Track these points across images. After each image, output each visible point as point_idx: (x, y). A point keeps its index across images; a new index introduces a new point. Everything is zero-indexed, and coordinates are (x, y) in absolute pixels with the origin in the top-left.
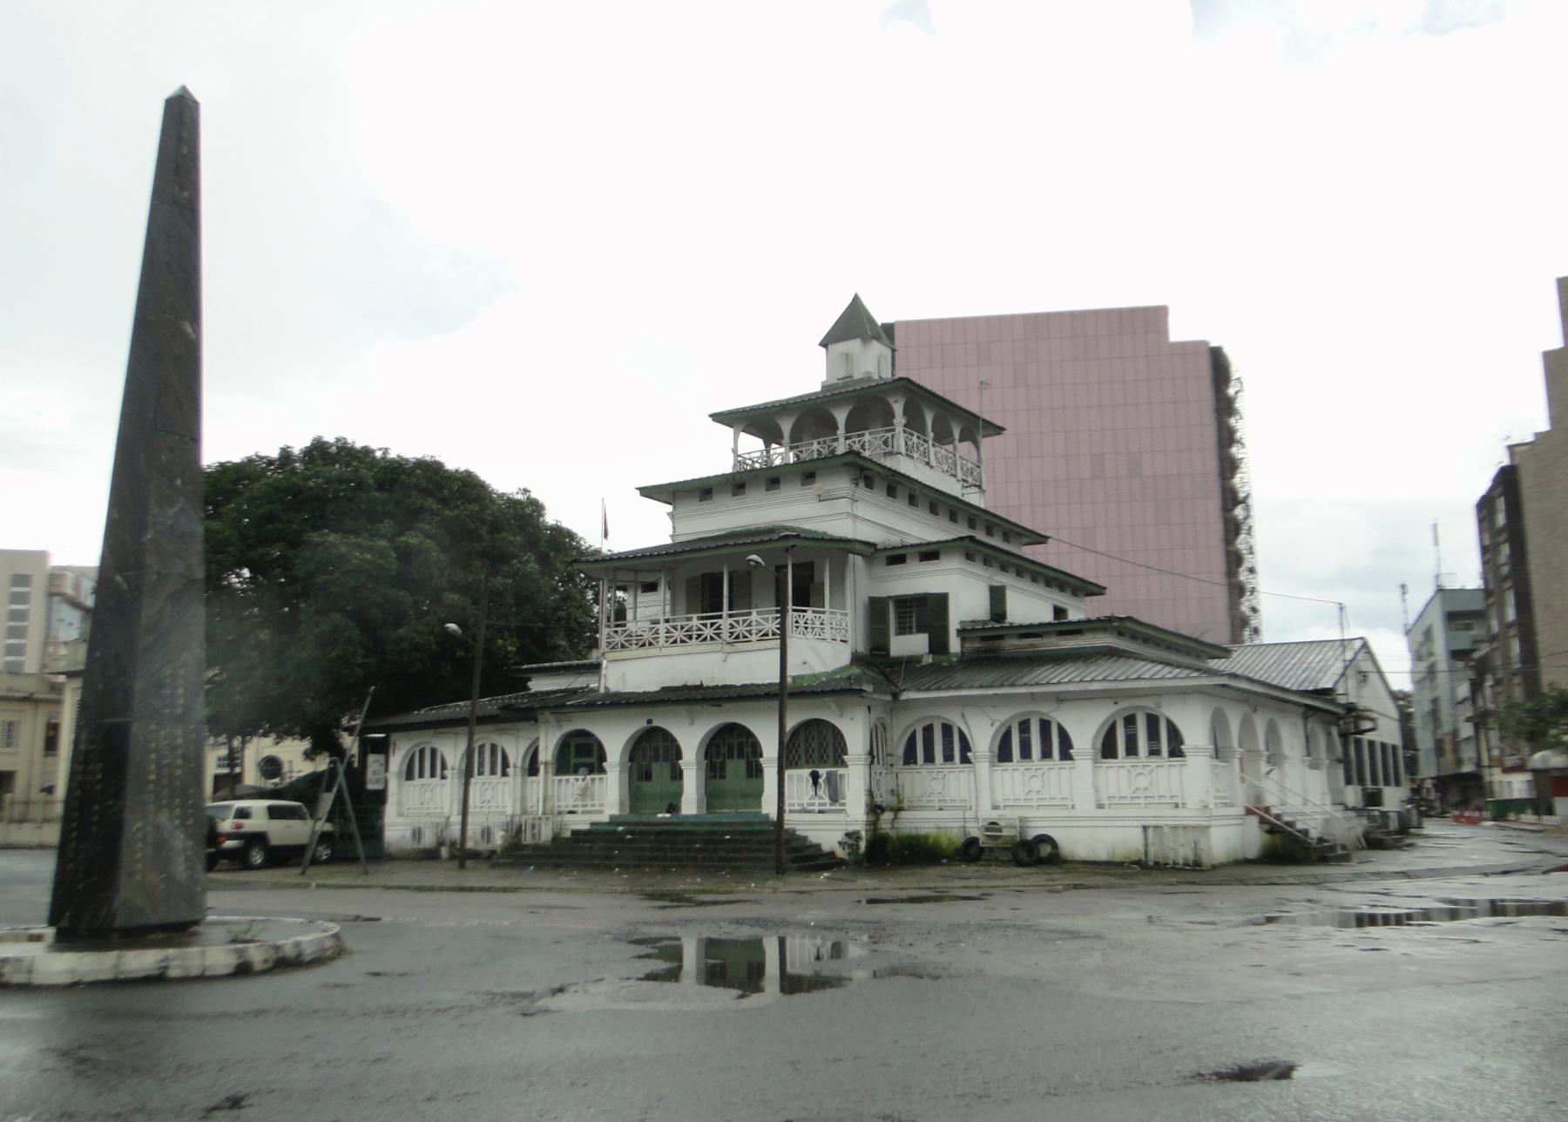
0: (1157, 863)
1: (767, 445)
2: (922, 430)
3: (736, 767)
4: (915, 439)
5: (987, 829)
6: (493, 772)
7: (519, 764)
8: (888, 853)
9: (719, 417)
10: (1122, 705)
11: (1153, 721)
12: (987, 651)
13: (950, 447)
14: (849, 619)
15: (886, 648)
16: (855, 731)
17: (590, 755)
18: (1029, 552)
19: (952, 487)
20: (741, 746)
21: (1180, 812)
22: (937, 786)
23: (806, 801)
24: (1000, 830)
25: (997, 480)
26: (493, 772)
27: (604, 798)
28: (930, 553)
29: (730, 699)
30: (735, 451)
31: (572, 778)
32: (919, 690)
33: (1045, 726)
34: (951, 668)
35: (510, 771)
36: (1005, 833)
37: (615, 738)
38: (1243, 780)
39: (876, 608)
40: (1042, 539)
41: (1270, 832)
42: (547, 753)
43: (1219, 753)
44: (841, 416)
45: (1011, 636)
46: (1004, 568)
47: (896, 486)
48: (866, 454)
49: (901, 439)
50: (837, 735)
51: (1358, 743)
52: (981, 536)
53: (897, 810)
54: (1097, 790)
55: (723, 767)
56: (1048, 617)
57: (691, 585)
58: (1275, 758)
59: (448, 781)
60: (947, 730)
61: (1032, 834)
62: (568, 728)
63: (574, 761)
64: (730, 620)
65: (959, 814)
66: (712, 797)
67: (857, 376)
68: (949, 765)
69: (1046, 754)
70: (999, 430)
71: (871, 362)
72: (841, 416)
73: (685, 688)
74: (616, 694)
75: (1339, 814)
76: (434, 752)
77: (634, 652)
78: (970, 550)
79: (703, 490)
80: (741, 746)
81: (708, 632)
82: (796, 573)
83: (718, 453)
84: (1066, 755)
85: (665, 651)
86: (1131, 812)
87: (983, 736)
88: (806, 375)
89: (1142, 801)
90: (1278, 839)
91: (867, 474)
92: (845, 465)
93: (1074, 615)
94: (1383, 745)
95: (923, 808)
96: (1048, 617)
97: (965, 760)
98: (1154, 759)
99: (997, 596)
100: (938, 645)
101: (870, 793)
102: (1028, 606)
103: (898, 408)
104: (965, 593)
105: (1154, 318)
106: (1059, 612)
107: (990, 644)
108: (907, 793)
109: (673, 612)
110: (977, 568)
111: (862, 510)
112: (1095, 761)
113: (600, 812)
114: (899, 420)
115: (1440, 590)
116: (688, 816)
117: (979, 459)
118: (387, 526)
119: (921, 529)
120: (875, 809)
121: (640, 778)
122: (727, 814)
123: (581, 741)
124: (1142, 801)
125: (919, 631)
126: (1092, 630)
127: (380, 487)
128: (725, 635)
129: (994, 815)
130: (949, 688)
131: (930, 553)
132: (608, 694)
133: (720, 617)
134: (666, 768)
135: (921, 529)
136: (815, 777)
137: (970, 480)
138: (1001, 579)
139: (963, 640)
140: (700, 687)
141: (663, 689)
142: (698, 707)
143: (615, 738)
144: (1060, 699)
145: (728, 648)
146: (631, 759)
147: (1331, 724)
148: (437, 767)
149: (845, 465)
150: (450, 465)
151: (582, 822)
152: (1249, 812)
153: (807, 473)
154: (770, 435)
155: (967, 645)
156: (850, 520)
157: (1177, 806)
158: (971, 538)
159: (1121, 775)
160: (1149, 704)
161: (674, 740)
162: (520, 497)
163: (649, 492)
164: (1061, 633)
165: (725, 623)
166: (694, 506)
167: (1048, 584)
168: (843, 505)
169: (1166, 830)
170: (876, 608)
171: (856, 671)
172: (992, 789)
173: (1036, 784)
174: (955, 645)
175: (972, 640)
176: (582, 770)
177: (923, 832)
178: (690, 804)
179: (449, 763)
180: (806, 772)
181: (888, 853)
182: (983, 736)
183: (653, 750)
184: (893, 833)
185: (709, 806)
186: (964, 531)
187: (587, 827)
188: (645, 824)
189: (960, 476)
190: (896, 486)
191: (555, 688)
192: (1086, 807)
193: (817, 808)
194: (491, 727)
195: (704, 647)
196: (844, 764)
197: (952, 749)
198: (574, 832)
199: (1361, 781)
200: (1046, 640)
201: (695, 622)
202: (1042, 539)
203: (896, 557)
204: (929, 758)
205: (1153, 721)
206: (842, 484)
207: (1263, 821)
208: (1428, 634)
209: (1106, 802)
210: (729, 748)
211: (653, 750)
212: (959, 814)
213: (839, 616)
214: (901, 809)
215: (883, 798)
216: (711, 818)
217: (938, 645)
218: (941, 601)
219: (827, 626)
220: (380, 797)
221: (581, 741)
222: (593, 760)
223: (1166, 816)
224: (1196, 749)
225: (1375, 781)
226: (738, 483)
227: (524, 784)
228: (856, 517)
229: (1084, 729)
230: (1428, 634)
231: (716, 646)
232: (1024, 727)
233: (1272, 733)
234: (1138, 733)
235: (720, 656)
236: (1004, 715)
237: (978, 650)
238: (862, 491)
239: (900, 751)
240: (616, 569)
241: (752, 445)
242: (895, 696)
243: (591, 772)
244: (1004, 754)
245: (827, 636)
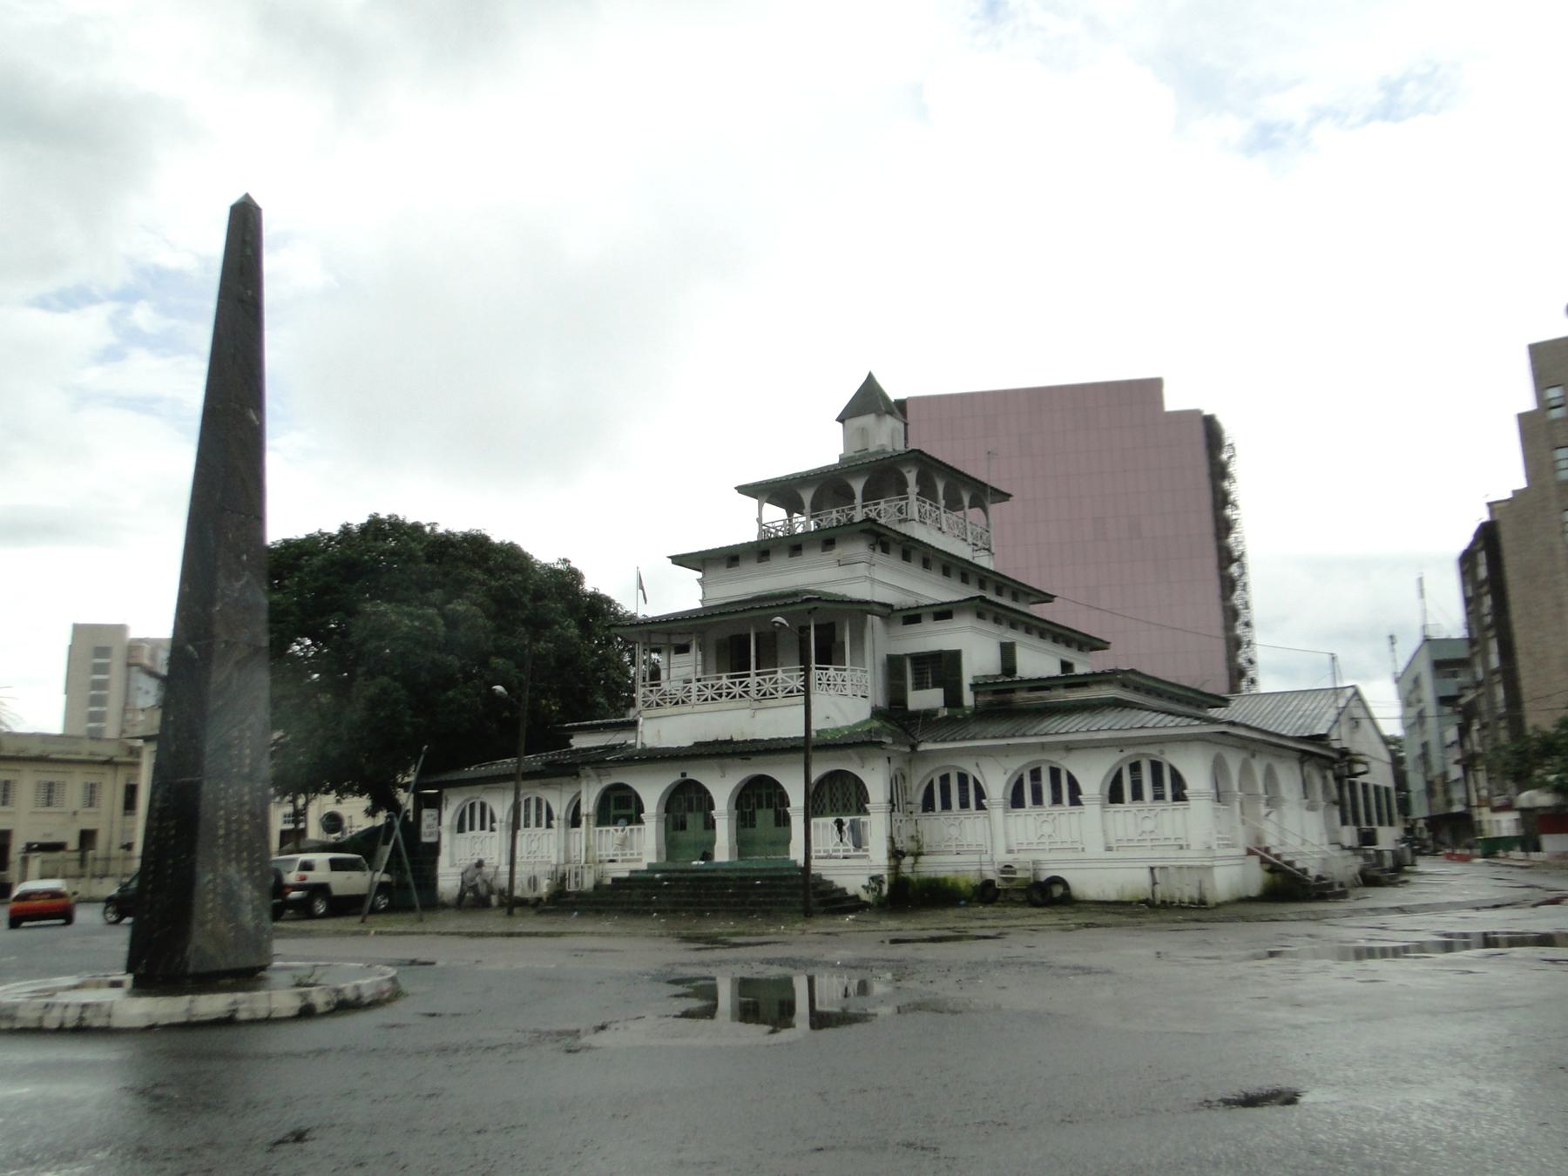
0: (1163, 902)
1: (790, 514)
2: (934, 499)
3: (765, 816)
4: (927, 507)
5: (1003, 872)
6: (538, 824)
8: (909, 895)
9: (745, 490)
10: (1128, 752)
11: (1156, 768)
12: (1001, 703)
13: (960, 514)
14: (868, 676)
15: (904, 703)
16: (876, 780)
17: (628, 807)
18: (1037, 610)
19: (962, 551)
20: (769, 797)
21: (1182, 853)
22: (954, 831)
23: (831, 847)
24: (1014, 872)
25: (1003, 543)
26: (538, 824)
27: (641, 847)
28: (943, 613)
29: (758, 753)
30: (759, 520)
31: (611, 829)
32: (935, 741)
33: (1055, 773)
34: (965, 721)
35: (554, 823)
36: (1019, 875)
37: (651, 791)
38: (1243, 822)
39: (894, 666)
40: (1047, 598)
41: (1270, 871)
42: (588, 806)
43: (1220, 797)
44: (858, 486)
45: (1022, 689)
46: (1013, 626)
47: (911, 550)
48: (882, 521)
49: (914, 506)
50: (860, 785)
51: (1352, 785)
52: (991, 596)
53: (917, 854)
54: (1105, 832)
55: (753, 818)
56: (1056, 671)
58: (1273, 801)
59: (496, 834)
60: (963, 778)
61: (1044, 876)
62: (607, 782)
63: (613, 812)
64: (758, 679)
65: (975, 858)
66: (743, 845)
67: (872, 450)
68: (965, 811)
70: (1005, 496)
71: (885, 436)
72: (858, 486)
73: (716, 742)
75: (1335, 852)
76: (483, 806)
77: (668, 709)
78: (982, 609)
79: (729, 558)
80: (769, 797)
81: (737, 690)
82: (820, 631)
83: (743, 523)
84: (1075, 800)
85: (697, 708)
86: (1137, 854)
87: (996, 784)
88: (822, 446)
89: (1148, 843)
90: (1278, 878)
91: (882, 539)
92: (863, 531)
93: (1080, 669)
94: (1377, 788)
95: (942, 853)
96: (1056, 671)
97: (980, 807)
98: (1160, 804)
99: (1007, 651)
100: (953, 699)
101: (892, 839)
102: (1037, 661)
103: (911, 477)
104: (977, 649)
105: (1152, 388)
106: (1066, 666)
108: (926, 840)
109: (704, 672)
110: (988, 626)
111: (879, 574)
112: (1103, 806)
113: (639, 860)
114: (913, 489)
115: (1427, 640)
116: (720, 863)
117: (988, 525)
118: (436, 595)
119: (934, 590)
120: (896, 854)
121: (676, 828)
122: (759, 861)
123: (624, 793)
124: (1148, 843)
125: (935, 685)
126: (1099, 683)
127: (430, 559)
128: (753, 693)
129: (1008, 859)
130: (964, 739)
131: (943, 613)
132: (644, 750)
135: (934, 590)
136: (840, 824)
137: (980, 544)
138: (1010, 636)
139: (976, 694)
140: (730, 742)
141: (697, 744)
142: (728, 761)
143: (651, 791)
144: (1069, 747)
145: (756, 705)
146: (667, 810)
147: (1326, 768)
148: (487, 820)
149: (863, 531)
150: (496, 539)
151: (622, 870)
152: (1250, 852)
153: (827, 540)
154: (793, 506)
155: (980, 698)
156: (867, 584)
157: (1181, 847)
158: (982, 598)
159: (1126, 818)
160: (1153, 751)
161: (707, 792)
162: (560, 567)
163: (679, 560)
164: (1069, 686)
165: (752, 681)
166: (723, 572)
167: (1055, 640)
168: (861, 569)
169: (1172, 870)
170: (894, 666)
171: (876, 724)
172: (1006, 834)
173: (1047, 829)
174: (968, 699)
175: (984, 693)
176: (622, 821)
177: (941, 875)
178: (723, 852)
179: (498, 816)
180: (831, 820)
181: (909, 895)
182: (996, 784)
183: (687, 803)
184: (914, 877)
185: (741, 854)
186: (976, 592)
187: (627, 875)
188: (682, 871)
189: (970, 540)
190: (911, 550)
192: (1095, 849)
193: (841, 854)
194: (537, 782)
195: (733, 704)
196: (866, 812)
198: (614, 880)
199: (1356, 821)
200: (1055, 693)
201: (725, 681)
202: (1047, 598)
203: (912, 617)
204: (946, 805)
205: (1156, 768)
206: (860, 549)
207: (1263, 861)
208: (1416, 682)
209: (1114, 845)
210: (759, 798)
211: (687, 803)
212: (975, 858)
213: (859, 674)
214: (921, 854)
215: (904, 844)
216: (742, 864)
217: (953, 699)
218: (954, 658)
219: (848, 683)
220: (434, 849)
221: (617, 794)
222: (632, 811)
223: (1171, 857)
224: (1199, 794)
225: (1369, 822)
226: (763, 550)
227: (567, 834)
228: (873, 580)
229: (1092, 776)
230: (1416, 682)
232: (1036, 775)
233: (1270, 775)
234: (1143, 779)
235: (748, 712)
236: (1016, 764)
237: (990, 703)
238: (878, 556)
239: (919, 798)
240: (651, 632)
241: (775, 514)
242: (913, 747)
243: (629, 823)
244: (1017, 801)
245: (848, 691)
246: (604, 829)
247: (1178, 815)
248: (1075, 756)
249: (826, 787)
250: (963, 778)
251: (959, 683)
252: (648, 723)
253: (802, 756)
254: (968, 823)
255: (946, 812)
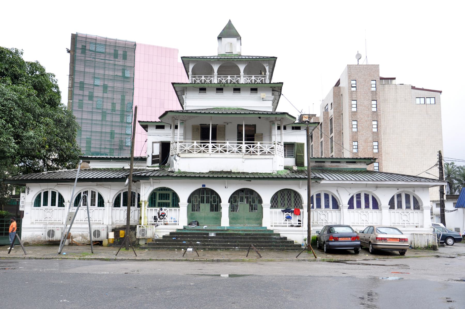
7: (111, 201)
12: (319, 167)
22: (322, 217)
27: (178, 218)
37: (184, 192)
50: (297, 195)
57: (194, 128)
63: (158, 201)
64: (247, 145)
66: (232, 219)
68: (327, 209)
69: (367, 206)
74: (184, 173)
77: (195, 154)
85: (212, 156)
98: (408, 210)
107: (320, 164)
109: (185, 139)
132: (180, 172)
133: (242, 143)
134: (208, 206)
140: (230, 172)
141: (211, 172)
143: (184, 192)
144: (377, 187)
157: (416, 227)
160: (410, 191)
178: (225, 222)
185: (230, 223)
191: (104, 167)
195: (233, 155)
197: (328, 203)
201: (195, 144)
211: (205, 198)
231: (240, 155)
232: (358, 196)
236: (354, 192)
246: (154, 209)
247: (375, 214)
248: (379, 189)
249: (279, 195)
250: (326, 196)
251: (303, 157)
252: (181, 159)
253: (306, 182)
254: (330, 214)
255: (319, 209)
